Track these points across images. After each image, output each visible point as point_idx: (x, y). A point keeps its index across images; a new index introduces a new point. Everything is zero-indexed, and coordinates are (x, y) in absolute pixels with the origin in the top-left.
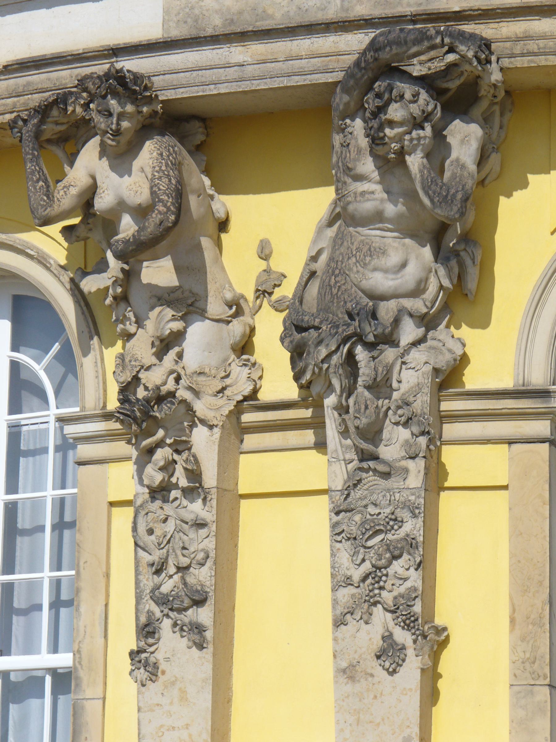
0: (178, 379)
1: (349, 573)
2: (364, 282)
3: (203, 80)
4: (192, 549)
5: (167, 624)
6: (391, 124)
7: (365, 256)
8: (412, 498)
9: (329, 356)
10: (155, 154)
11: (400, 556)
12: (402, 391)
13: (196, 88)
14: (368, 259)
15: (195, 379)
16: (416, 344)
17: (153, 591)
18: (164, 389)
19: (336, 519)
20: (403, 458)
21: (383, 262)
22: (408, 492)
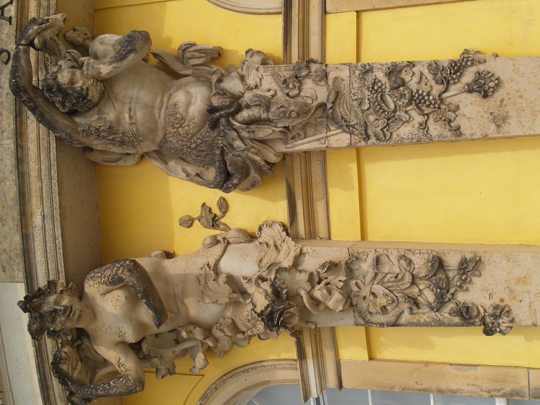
0: (264, 280)
1: (417, 125)
2: (196, 120)
3: (52, 248)
4: (397, 270)
5: (461, 297)
6: (72, 82)
7: (177, 118)
8: (357, 72)
9: (242, 139)
10: (91, 283)
11: (403, 80)
12: (277, 88)
13: (58, 255)
14: (178, 116)
15: (263, 265)
16: (242, 78)
17: (432, 309)
18: (269, 290)
19: (373, 140)
20: (327, 83)
21: (182, 104)
22: (353, 76)
